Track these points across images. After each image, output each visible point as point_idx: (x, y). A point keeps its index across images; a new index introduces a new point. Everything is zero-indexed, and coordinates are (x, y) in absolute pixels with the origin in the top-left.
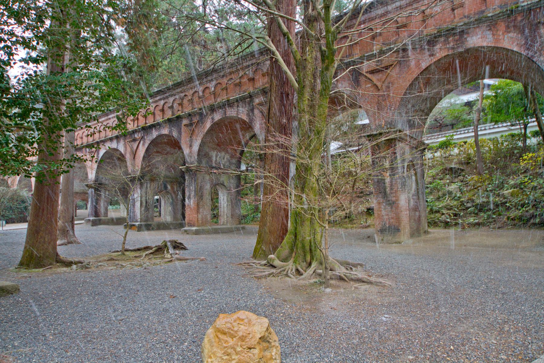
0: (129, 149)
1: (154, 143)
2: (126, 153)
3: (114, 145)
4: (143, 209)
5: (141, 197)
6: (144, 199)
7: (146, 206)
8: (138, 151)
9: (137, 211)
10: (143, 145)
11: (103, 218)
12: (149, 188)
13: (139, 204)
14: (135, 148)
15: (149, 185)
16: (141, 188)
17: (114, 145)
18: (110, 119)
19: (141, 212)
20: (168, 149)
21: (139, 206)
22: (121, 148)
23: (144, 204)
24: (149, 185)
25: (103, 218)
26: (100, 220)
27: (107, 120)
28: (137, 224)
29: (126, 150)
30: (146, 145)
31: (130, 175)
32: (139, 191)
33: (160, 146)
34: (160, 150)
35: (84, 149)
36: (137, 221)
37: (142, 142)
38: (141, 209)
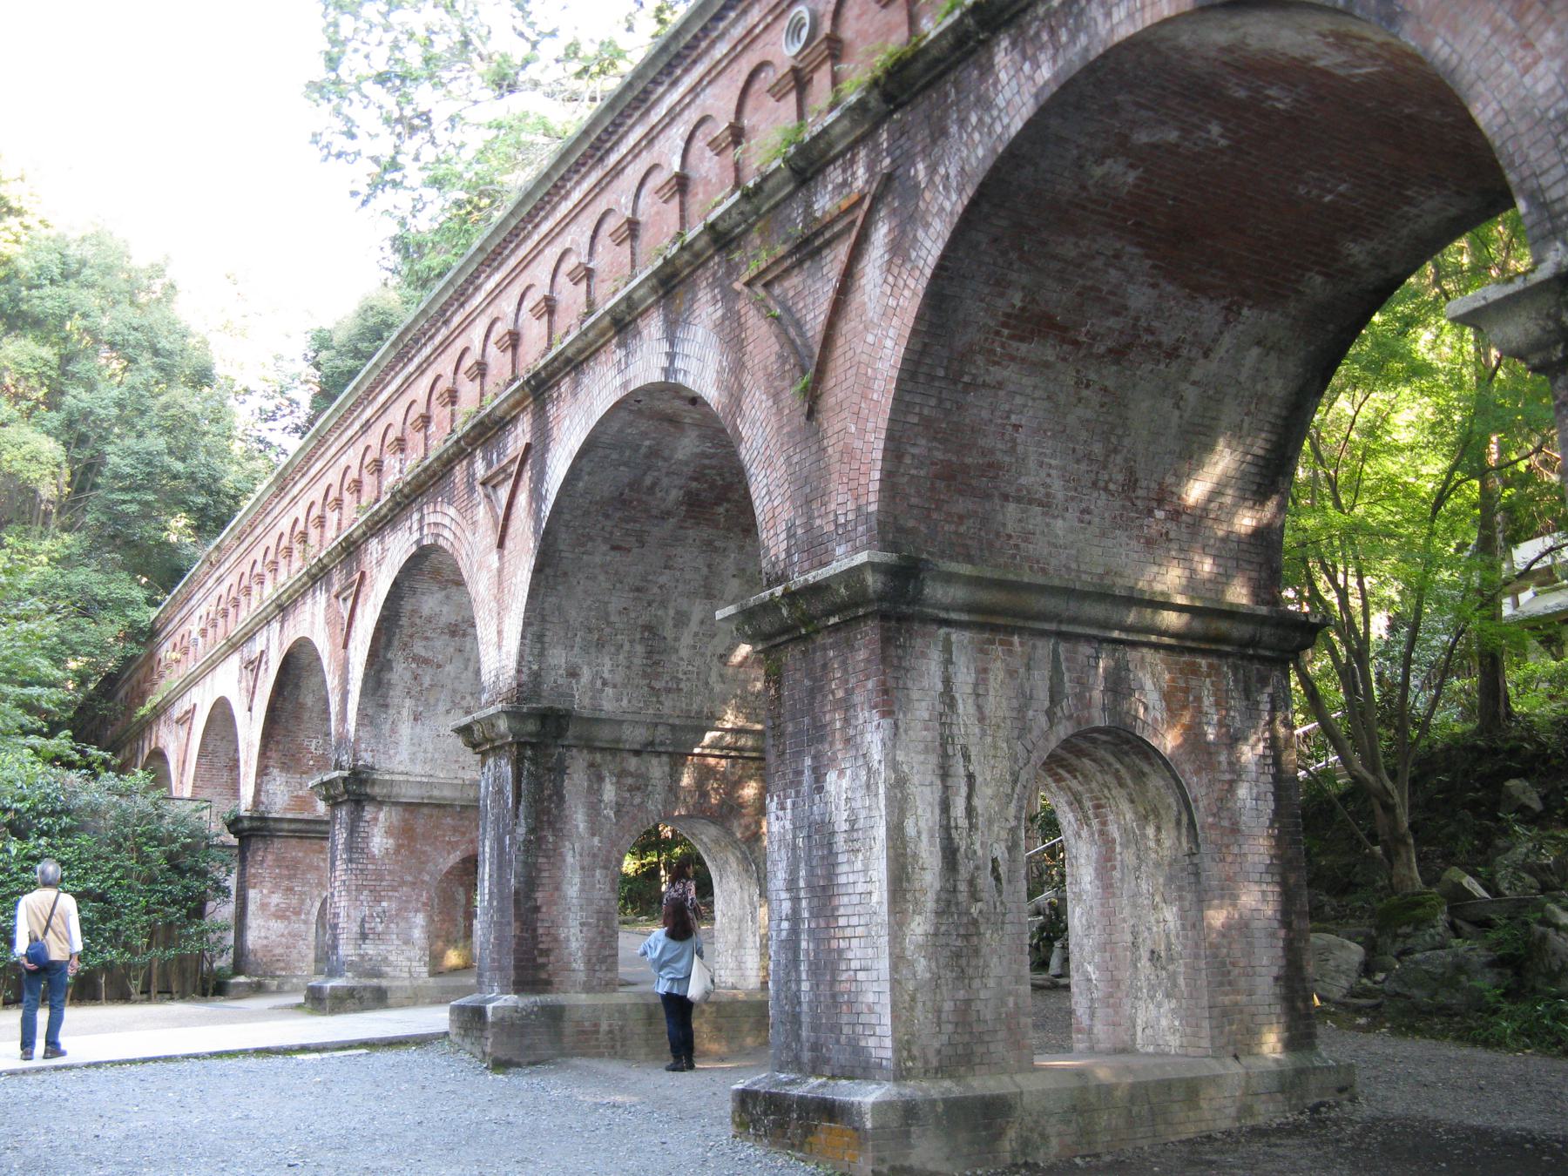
0: (763, 344)
1: (1007, 205)
2: (735, 398)
3: (644, 362)
4: (919, 927)
5: (899, 805)
6: (923, 821)
7: (947, 904)
8: (846, 328)
9: (856, 953)
10: (899, 249)
11: (583, 999)
12: (965, 707)
13: (880, 870)
14: (815, 318)
15: (964, 678)
16: (890, 702)
17: (644, 362)
18: (617, 171)
19: (898, 960)
20: (1139, 298)
21: (880, 895)
22: (702, 372)
23: (929, 875)
24: (964, 678)
25: (583, 999)
26: (554, 1015)
27: (600, 188)
28: (867, 1096)
29: (737, 368)
30: (931, 246)
31: (781, 579)
32: (874, 740)
33: (1069, 248)
34: (1056, 298)
35: (459, 472)
36: (862, 1069)
37: (881, 234)
38: (896, 936)
